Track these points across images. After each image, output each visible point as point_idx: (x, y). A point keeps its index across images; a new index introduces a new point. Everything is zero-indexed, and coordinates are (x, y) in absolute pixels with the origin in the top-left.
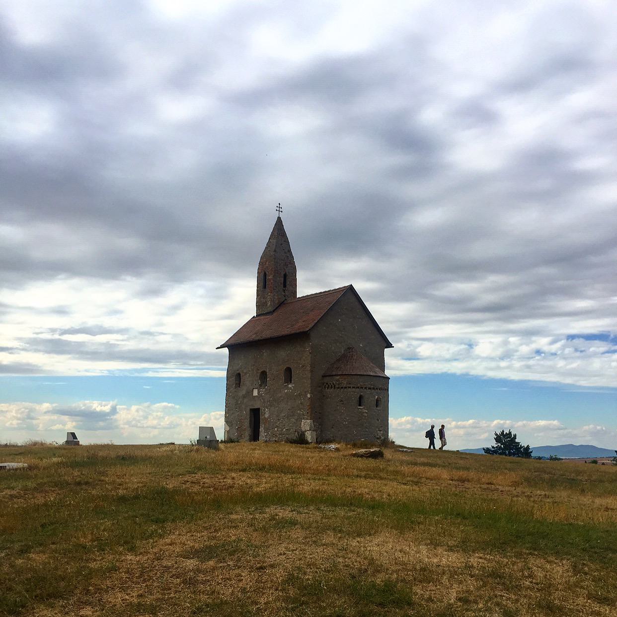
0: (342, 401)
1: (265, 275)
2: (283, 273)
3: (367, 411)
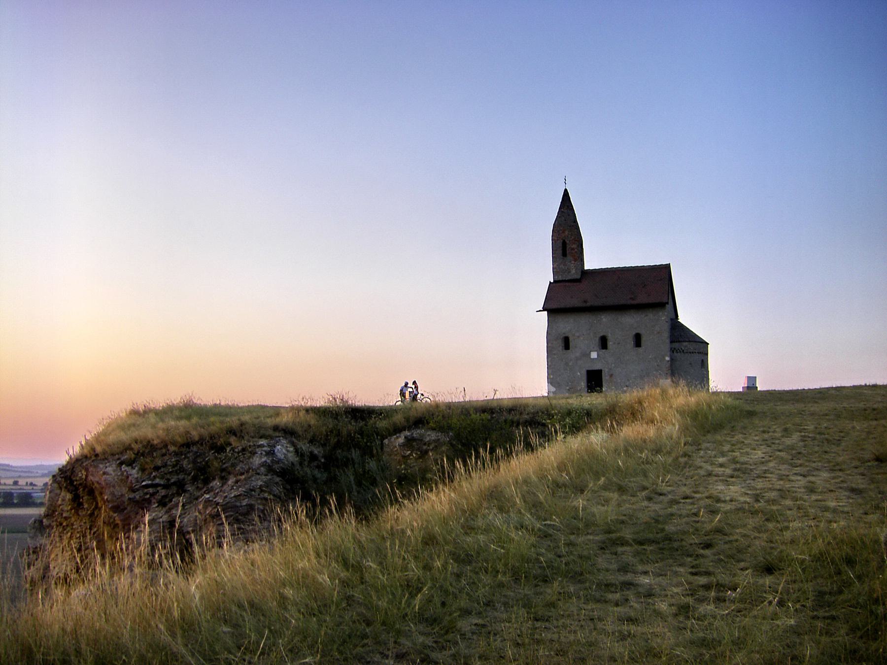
1: (564, 244)
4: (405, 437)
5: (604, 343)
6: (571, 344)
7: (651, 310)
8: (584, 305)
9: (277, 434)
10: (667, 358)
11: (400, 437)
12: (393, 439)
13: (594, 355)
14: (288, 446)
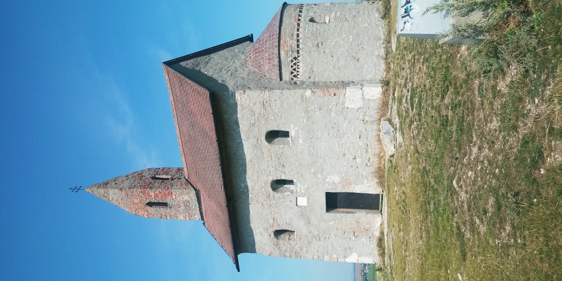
0: (318, 45)
1: (150, 204)
2: (151, 180)
3: (334, 13)
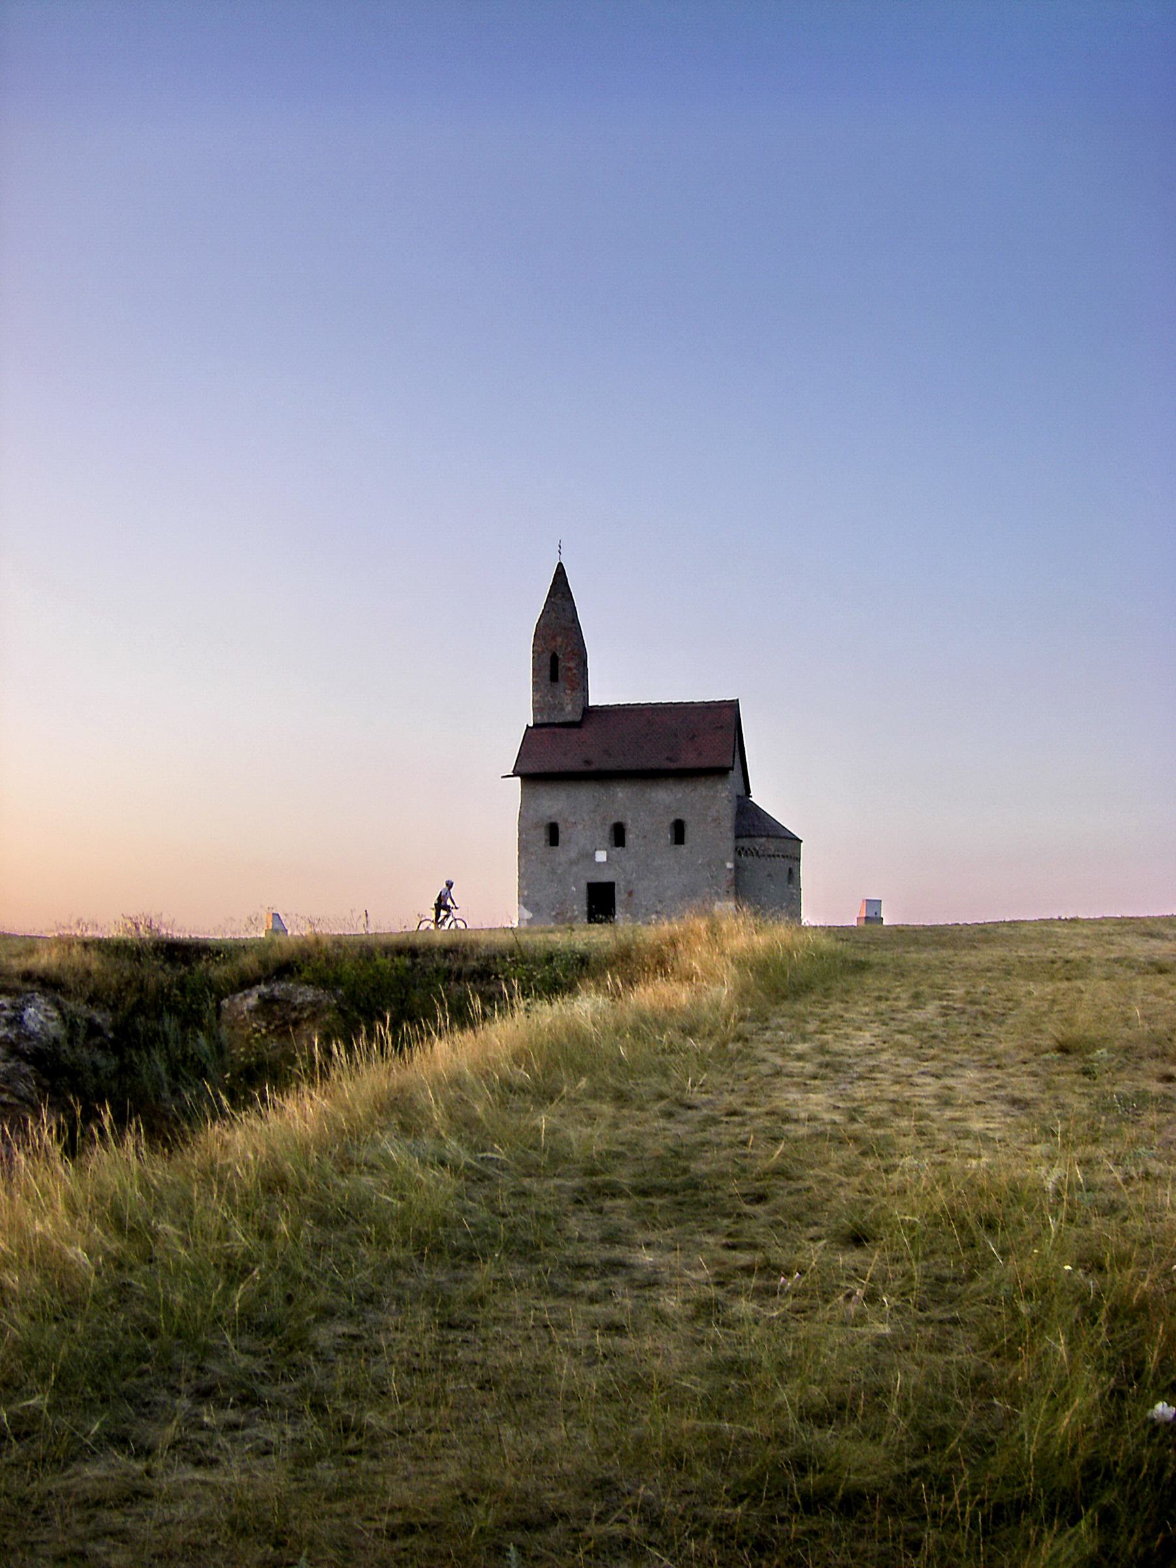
1: (554, 660)
4: (260, 996)
5: (618, 835)
6: (561, 837)
7: (703, 779)
8: (583, 768)
9: (29, 987)
10: (729, 865)
11: (250, 995)
12: (237, 1000)
13: (601, 856)
14: (49, 1008)
